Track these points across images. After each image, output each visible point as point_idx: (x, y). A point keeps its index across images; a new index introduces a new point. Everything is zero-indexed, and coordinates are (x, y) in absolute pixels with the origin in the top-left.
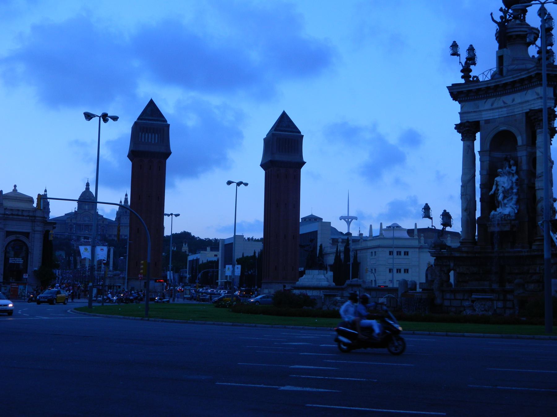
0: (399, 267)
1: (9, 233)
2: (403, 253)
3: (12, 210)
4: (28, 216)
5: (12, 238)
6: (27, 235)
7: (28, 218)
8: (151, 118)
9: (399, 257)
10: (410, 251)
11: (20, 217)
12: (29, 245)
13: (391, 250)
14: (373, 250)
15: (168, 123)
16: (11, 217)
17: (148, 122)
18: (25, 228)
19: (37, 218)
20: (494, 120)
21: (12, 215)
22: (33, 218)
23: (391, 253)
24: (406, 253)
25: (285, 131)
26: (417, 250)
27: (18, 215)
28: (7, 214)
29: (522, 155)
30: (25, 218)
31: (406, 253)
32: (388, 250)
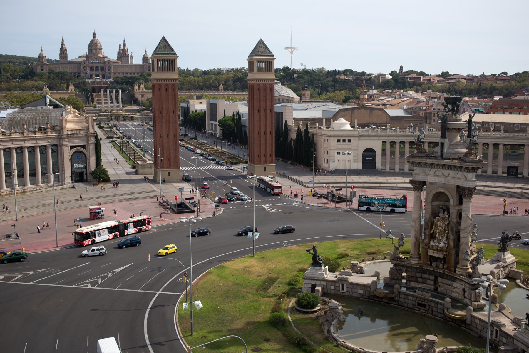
1: (72, 147)
2: (347, 141)
3: (72, 130)
5: (74, 150)
6: (84, 147)
9: (344, 143)
10: (352, 139)
13: (339, 139)
14: (326, 138)
20: (435, 183)
23: (339, 141)
24: (349, 141)
26: (357, 138)
29: (453, 211)
31: (349, 141)
32: (336, 139)
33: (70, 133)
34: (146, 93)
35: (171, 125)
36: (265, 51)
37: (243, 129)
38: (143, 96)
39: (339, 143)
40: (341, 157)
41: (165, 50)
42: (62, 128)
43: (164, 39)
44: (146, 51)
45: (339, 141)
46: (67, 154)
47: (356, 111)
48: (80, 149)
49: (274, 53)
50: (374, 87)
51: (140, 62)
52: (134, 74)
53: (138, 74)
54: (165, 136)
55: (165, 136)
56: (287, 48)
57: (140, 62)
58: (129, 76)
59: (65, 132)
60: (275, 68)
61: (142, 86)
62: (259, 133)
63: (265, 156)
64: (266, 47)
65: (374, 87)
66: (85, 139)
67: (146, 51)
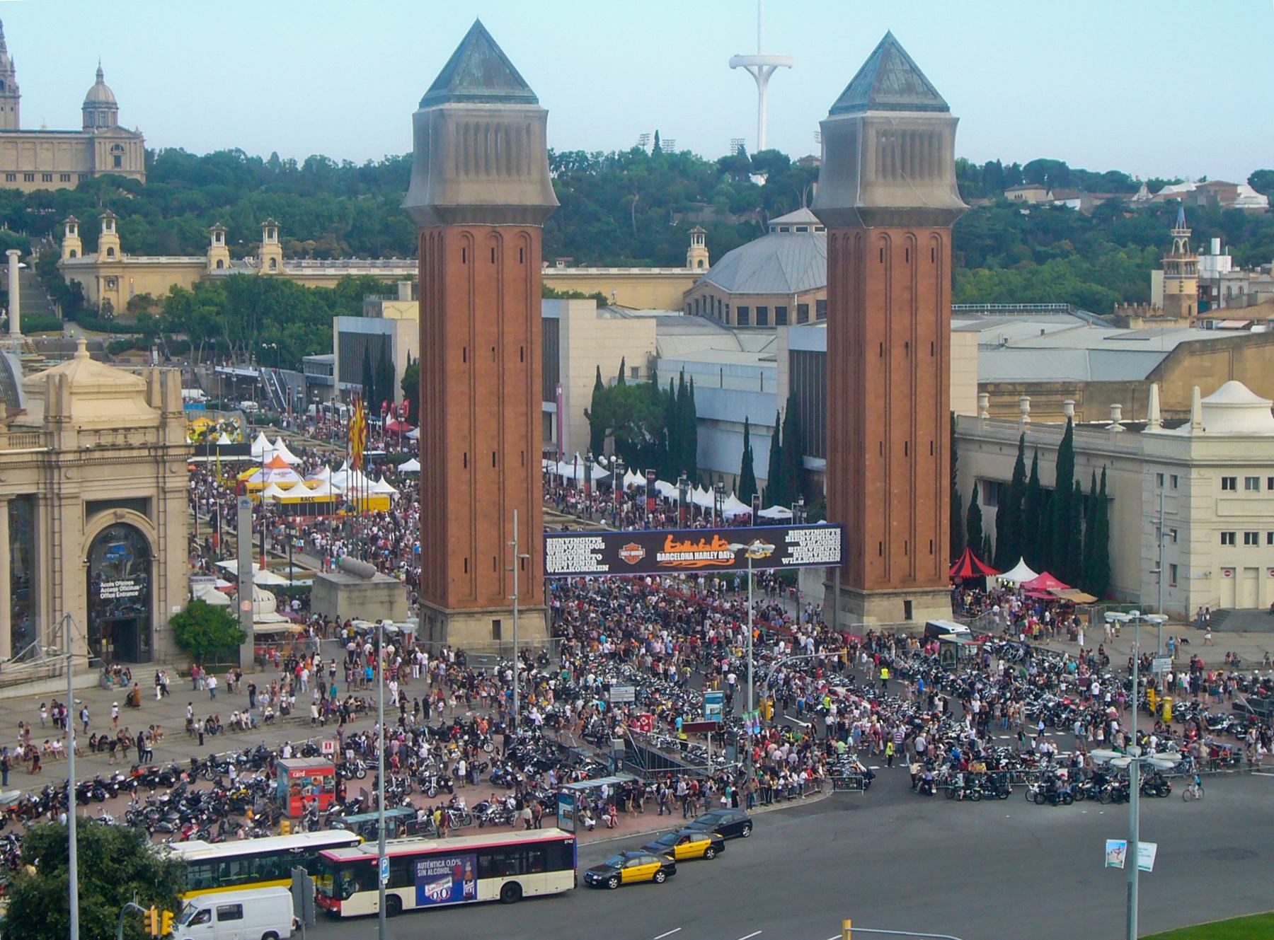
0: (1251, 528)
1: (93, 507)
4: (143, 446)
5: (105, 519)
6: (142, 504)
7: (145, 453)
8: (486, 92)
9: (1252, 494)
11: (123, 454)
12: (151, 535)
13: (1228, 473)
14: (1168, 473)
15: (543, 104)
16: (97, 455)
17: (480, 106)
18: (139, 484)
19: (172, 452)
21: (100, 448)
22: (160, 453)
23: (1229, 484)
25: (902, 107)
27: (115, 447)
28: (88, 450)
30: (135, 453)
32: (1217, 476)
33: (89, 443)
34: (126, 266)
35: (509, 412)
36: (909, 89)
37: (701, 431)
38: (112, 281)
39: (1228, 493)
40: (1240, 554)
41: (488, 82)
42: (56, 421)
43: (478, 36)
44: (100, 75)
45: (1229, 484)
46: (70, 538)
47: (1250, 353)
48: (132, 517)
49: (946, 95)
50: (1216, 243)
51: (74, 121)
52: (47, 177)
53: (65, 177)
54: (483, 462)
55: (483, 462)
56: (737, 62)
57: (74, 121)
58: (28, 188)
59: (69, 441)
60: (957, 156)
61: (109, 237)
62: (884, 449)
63: (909, 549)
64: (914, 70)
65: (1216, 243)
66: (148, 471)
67: (100, 75)
